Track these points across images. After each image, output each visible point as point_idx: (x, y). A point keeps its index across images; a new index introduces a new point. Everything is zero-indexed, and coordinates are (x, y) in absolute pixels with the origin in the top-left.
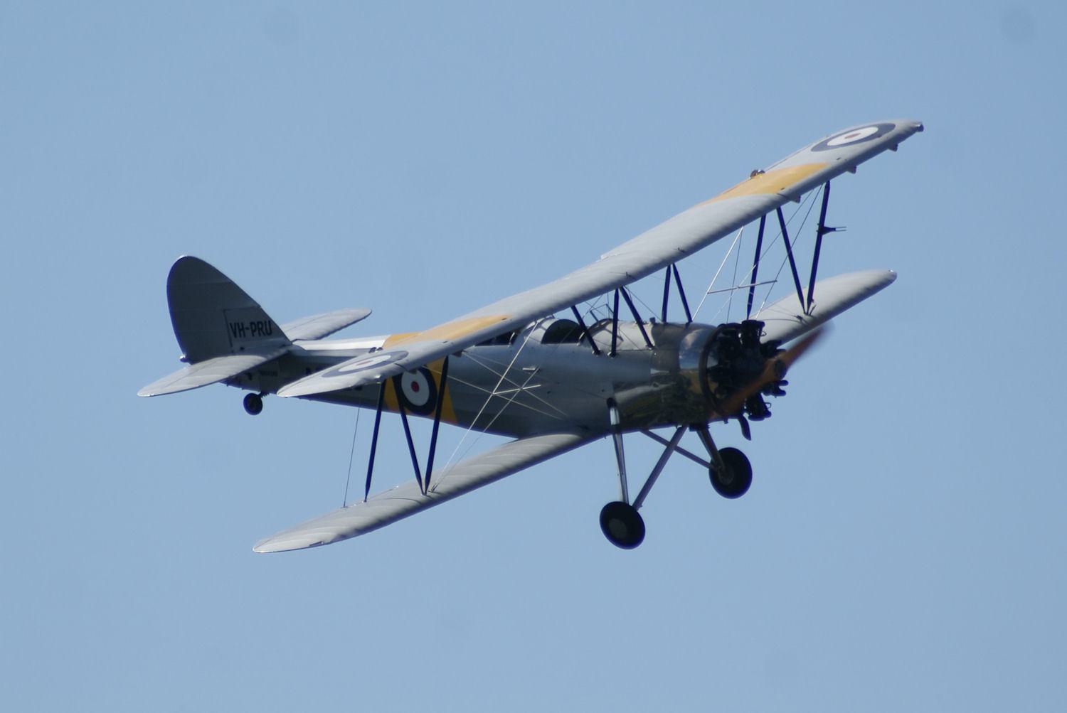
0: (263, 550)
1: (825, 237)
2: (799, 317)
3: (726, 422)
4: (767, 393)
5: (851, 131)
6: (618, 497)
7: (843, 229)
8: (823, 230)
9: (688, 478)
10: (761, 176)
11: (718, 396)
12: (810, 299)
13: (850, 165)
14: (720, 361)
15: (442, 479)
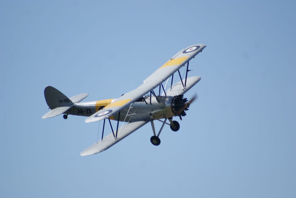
0: (83, 155)
1: (188, 72)
2: (183, 90)
3: (176, 116)
4: (185, 110)
5: (191, 47)
6: (153, 135)
7: (192, 70)
8: (188, 71)
9: (167, 127)
10: (173, 60)
11: (175, 112)
12: (185, 85)
13: (193, 57)
14: (175, 105)
15: (119, 136)
